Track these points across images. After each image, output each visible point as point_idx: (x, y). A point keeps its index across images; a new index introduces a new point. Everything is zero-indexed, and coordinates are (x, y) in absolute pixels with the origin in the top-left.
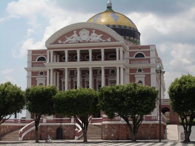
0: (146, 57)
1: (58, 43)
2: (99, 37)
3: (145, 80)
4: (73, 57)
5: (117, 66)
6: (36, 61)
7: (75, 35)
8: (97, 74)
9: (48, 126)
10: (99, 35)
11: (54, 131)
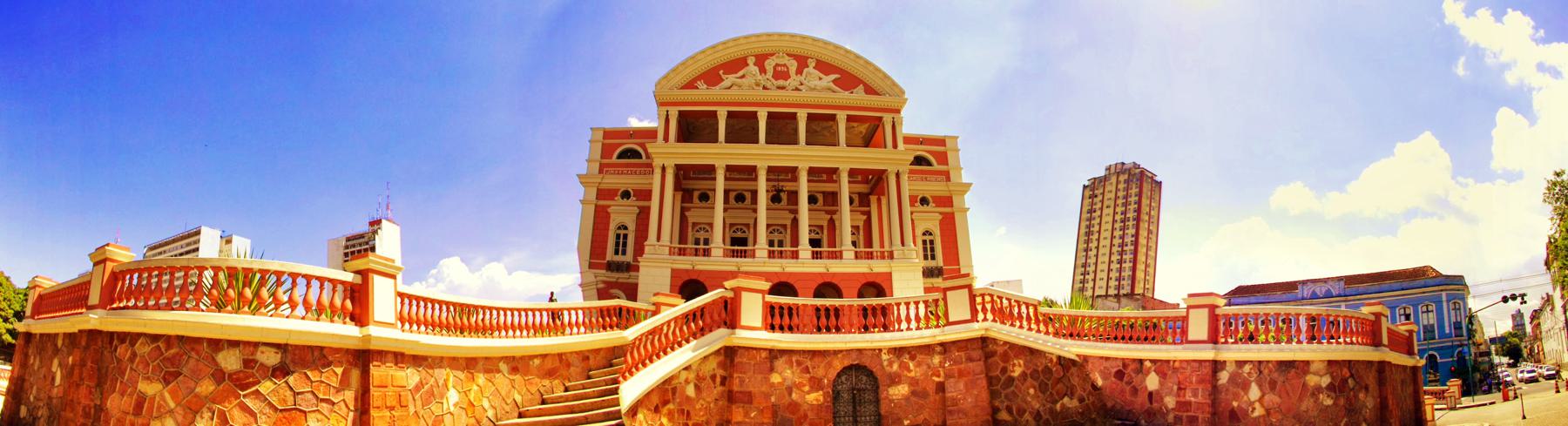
0: (936, 167)
2: (828, 80)
4: (742, 127)
5: (892, 169)
9: (774, 354)
11: (815, 397)
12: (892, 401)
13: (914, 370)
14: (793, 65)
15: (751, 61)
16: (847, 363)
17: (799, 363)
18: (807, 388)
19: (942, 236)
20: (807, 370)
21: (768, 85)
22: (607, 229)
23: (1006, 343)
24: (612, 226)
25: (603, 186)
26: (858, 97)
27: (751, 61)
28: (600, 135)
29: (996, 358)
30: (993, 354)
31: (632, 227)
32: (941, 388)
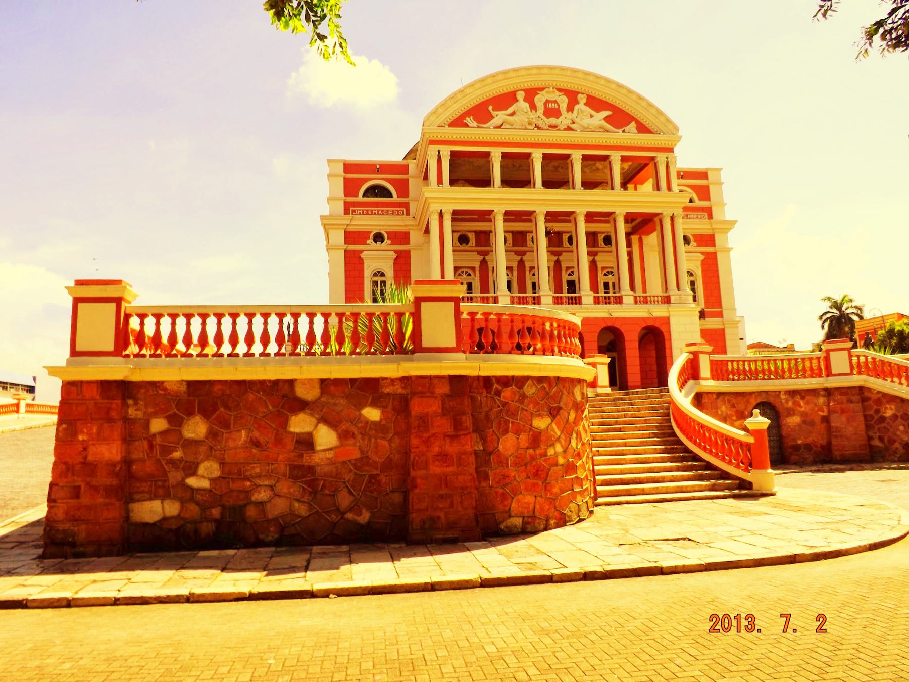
1: (467, 126)
3: (703, 271)
4: (517, 174)
5: (667, 213)
6: (360, 198)
7: (522, 104)
8: (560, 244)
10: (598, 110)
12: (789, 427)
13: (804, 407)
14: (563, 101)
15: (520, 96)
16: (759, 400)
17: (729, 401)
18: (734, 418)
19: (704, 276)
20: (733, 406)
21: (541, 124)
22: (362, 277)
23: (879, 392)
25: (351, 229)
26: (629, 136)
27: (520, 96)
28: (340, 169)
29: (870, 402)
30: (868, 399)
32: (826, 420)
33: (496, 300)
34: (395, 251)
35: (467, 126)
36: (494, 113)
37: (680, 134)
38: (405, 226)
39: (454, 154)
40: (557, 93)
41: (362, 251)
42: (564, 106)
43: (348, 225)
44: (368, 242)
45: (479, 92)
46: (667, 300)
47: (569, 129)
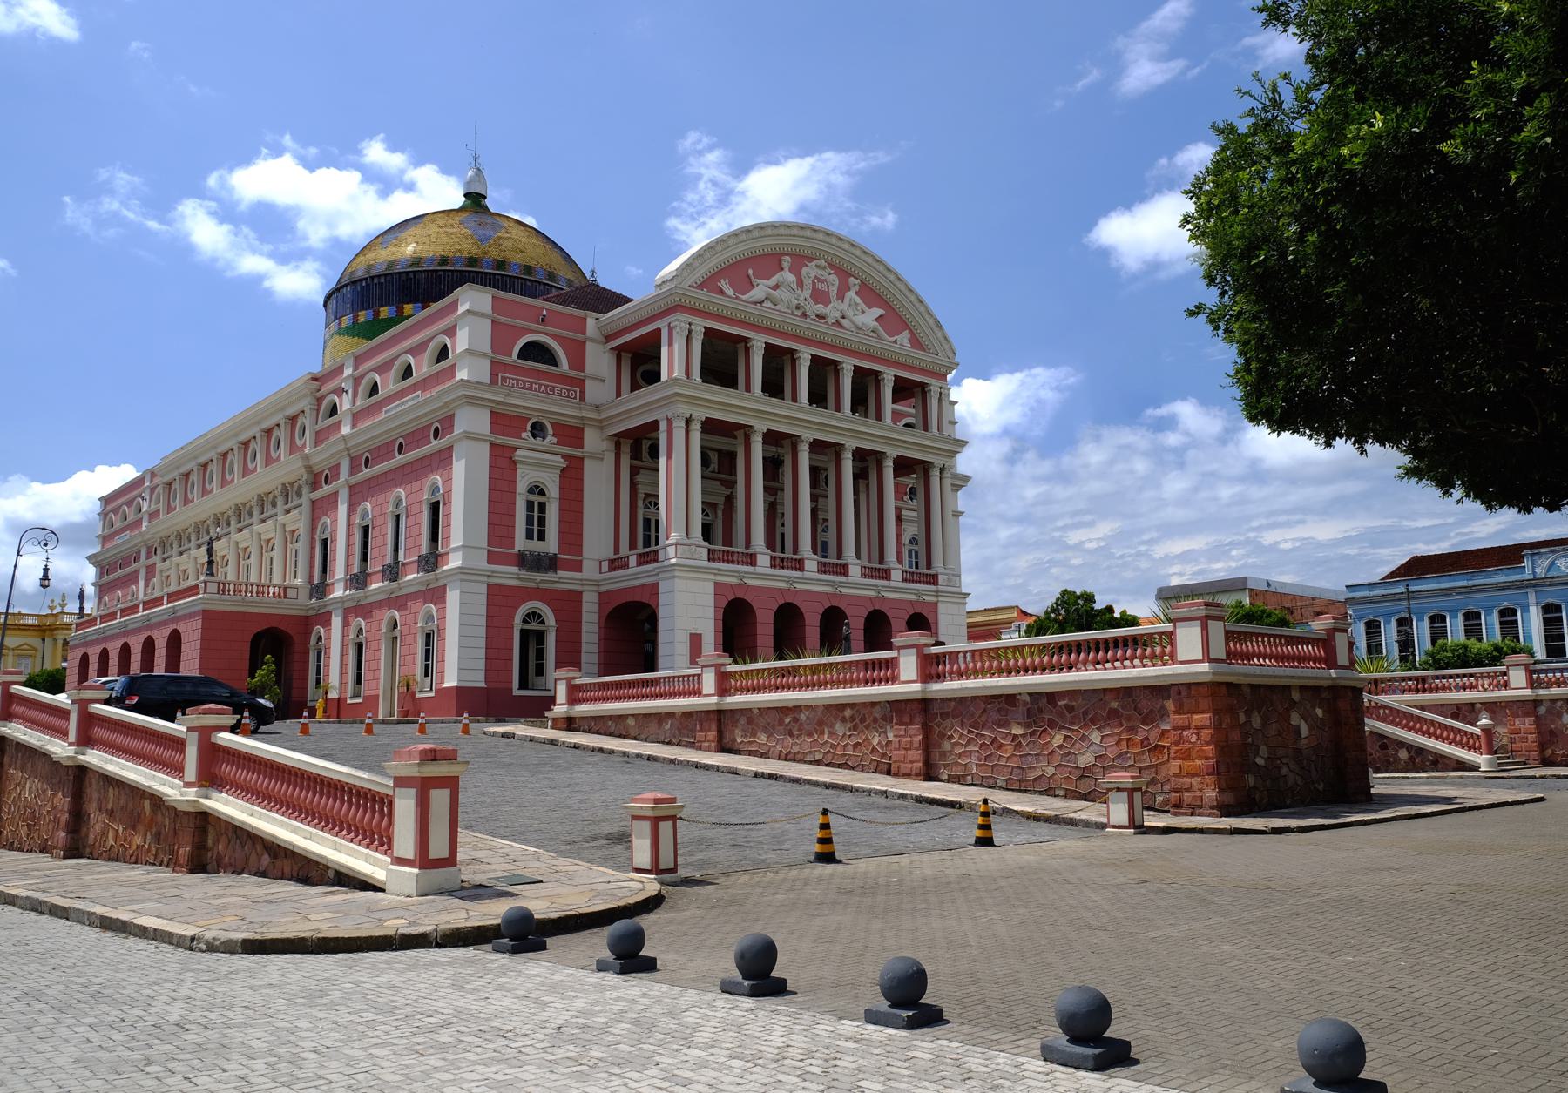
2: (869, 317)
5: (938, 461)
15: (786, 262)
24: (521, 487)
31: (553, 491)
33: (751, 560)
34: (564, 456)
35: (722, 292)
36: (755, 281)
37: (957, 359)
38: (582, 418)
39: (708, 332)
40: (829, 270)
41: (515, 449)
42: (834, 290)
43: (499, 403)
44: (524, 435)
45: (742, 248)
46: (933, 579)
47: (838, 324)
